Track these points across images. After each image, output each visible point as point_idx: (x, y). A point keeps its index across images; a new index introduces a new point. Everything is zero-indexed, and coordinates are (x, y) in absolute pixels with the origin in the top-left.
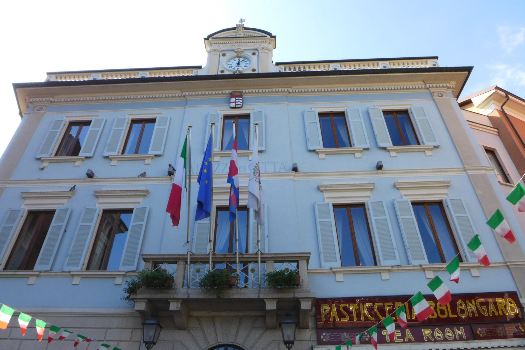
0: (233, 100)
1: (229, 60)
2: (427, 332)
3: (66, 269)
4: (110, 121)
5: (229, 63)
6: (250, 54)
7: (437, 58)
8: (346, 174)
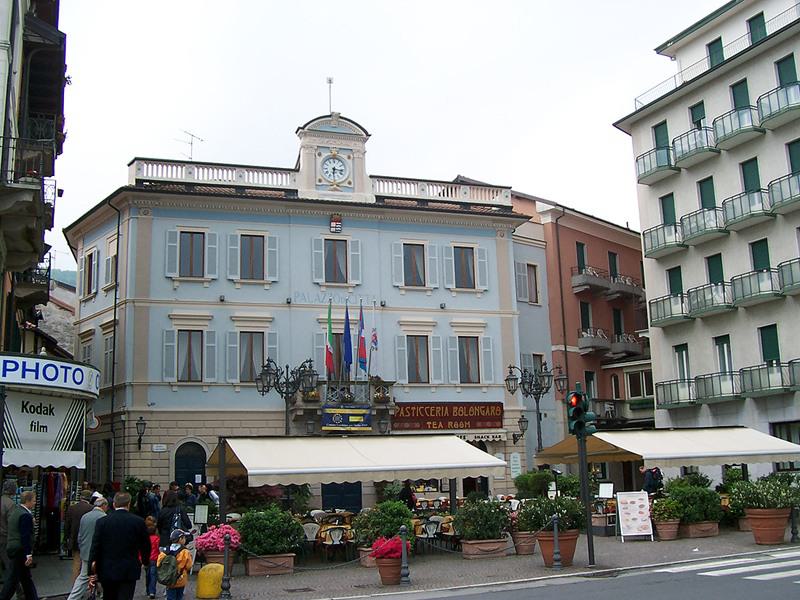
0: (333, 224)
1: (324, 162)
2: (450, 423)
3: (230, 381)
4: (223, 236)
5: (325, 166)
6: (345, 157)
7: (510, 188)
8: (418, 311)
